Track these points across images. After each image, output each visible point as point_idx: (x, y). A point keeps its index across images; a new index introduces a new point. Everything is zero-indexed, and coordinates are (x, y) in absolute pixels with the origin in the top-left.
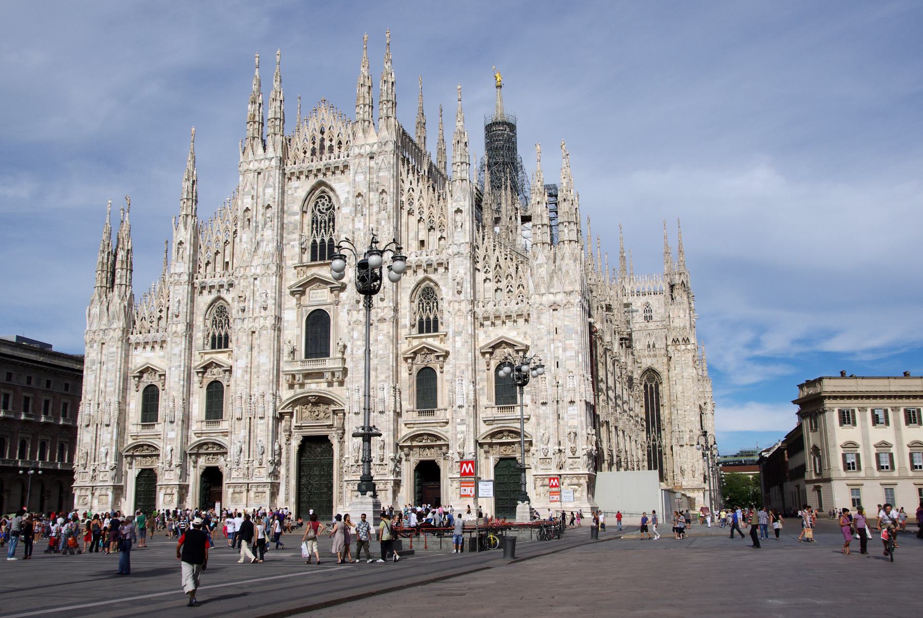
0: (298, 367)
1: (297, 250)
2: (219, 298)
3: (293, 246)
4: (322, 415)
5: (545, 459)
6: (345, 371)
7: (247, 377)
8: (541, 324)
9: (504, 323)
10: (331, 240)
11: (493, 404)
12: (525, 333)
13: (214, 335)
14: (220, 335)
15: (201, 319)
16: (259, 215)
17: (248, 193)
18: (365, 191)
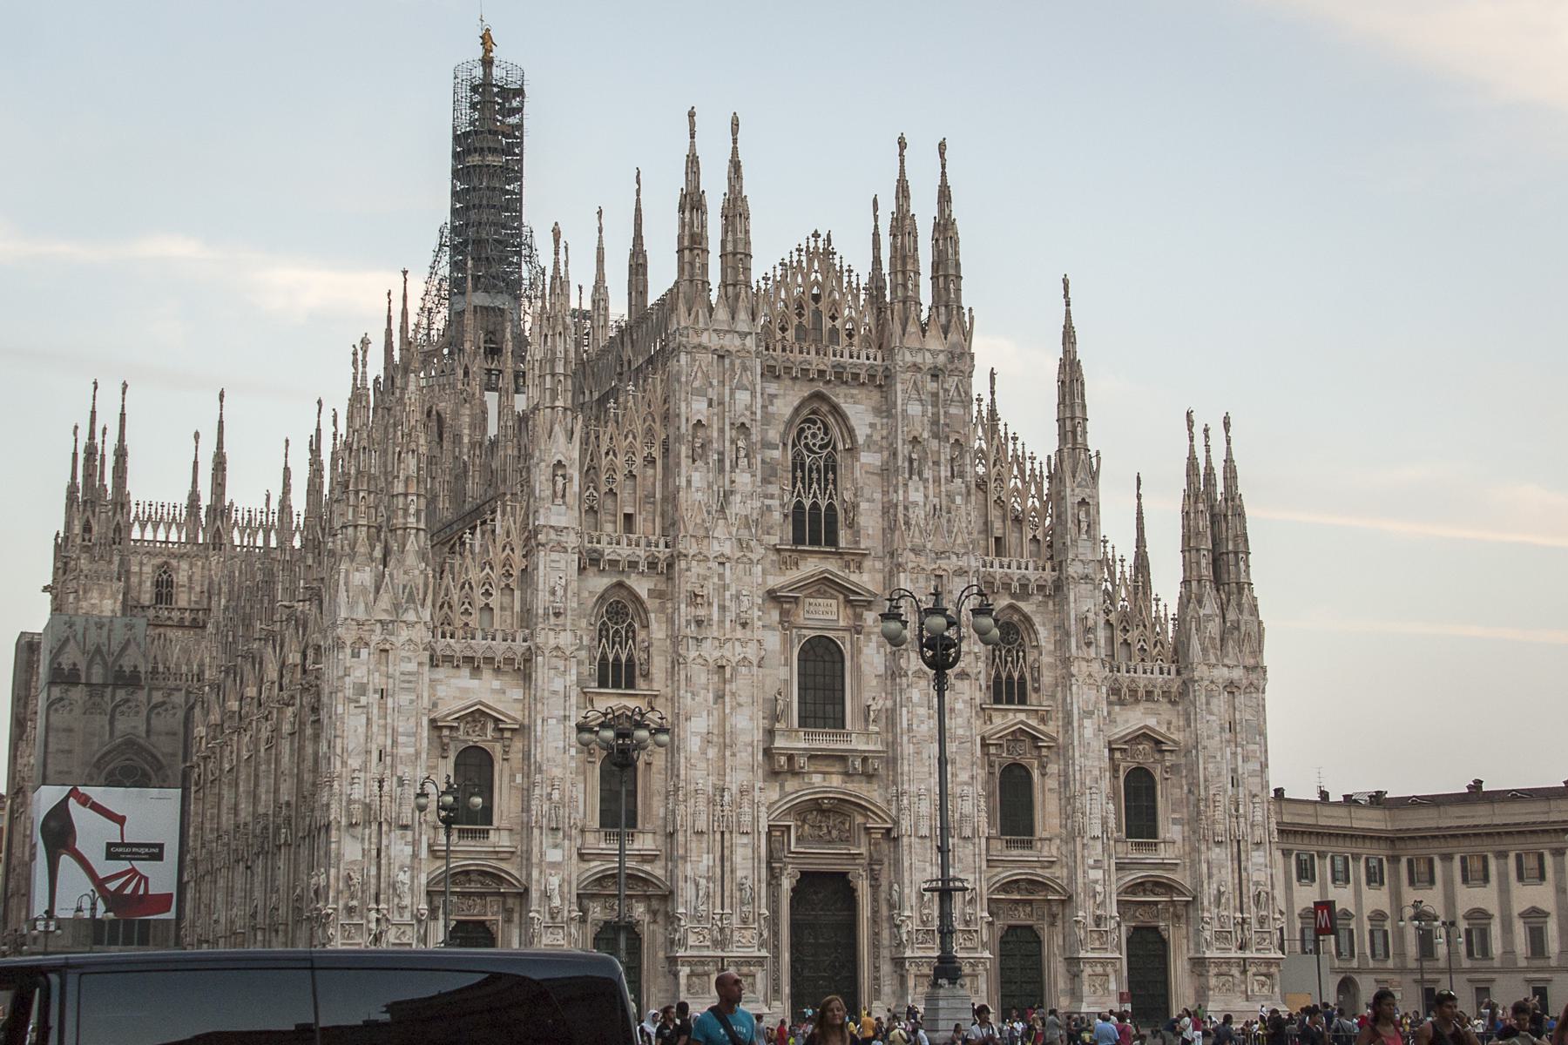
0: (800, 743)
1: (777, 516)
2: (620, 585)
3: (769, 507)
4: (835, 833)
5: (1222, 936)
6: (892, 761)
7: (712, 753)
8: (1211, 714)
9: (1137, 701)
10: (831, 507)
11: (1124, 835)
12: (1169, 723)
13: (604, 658)
14: (617, 659)
15: (584, 623)
16: (721, 439)
17: (700, 392)
18: (925, 435)
